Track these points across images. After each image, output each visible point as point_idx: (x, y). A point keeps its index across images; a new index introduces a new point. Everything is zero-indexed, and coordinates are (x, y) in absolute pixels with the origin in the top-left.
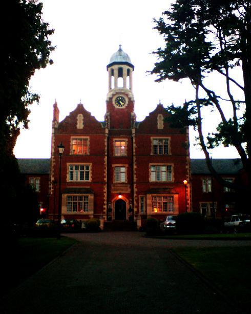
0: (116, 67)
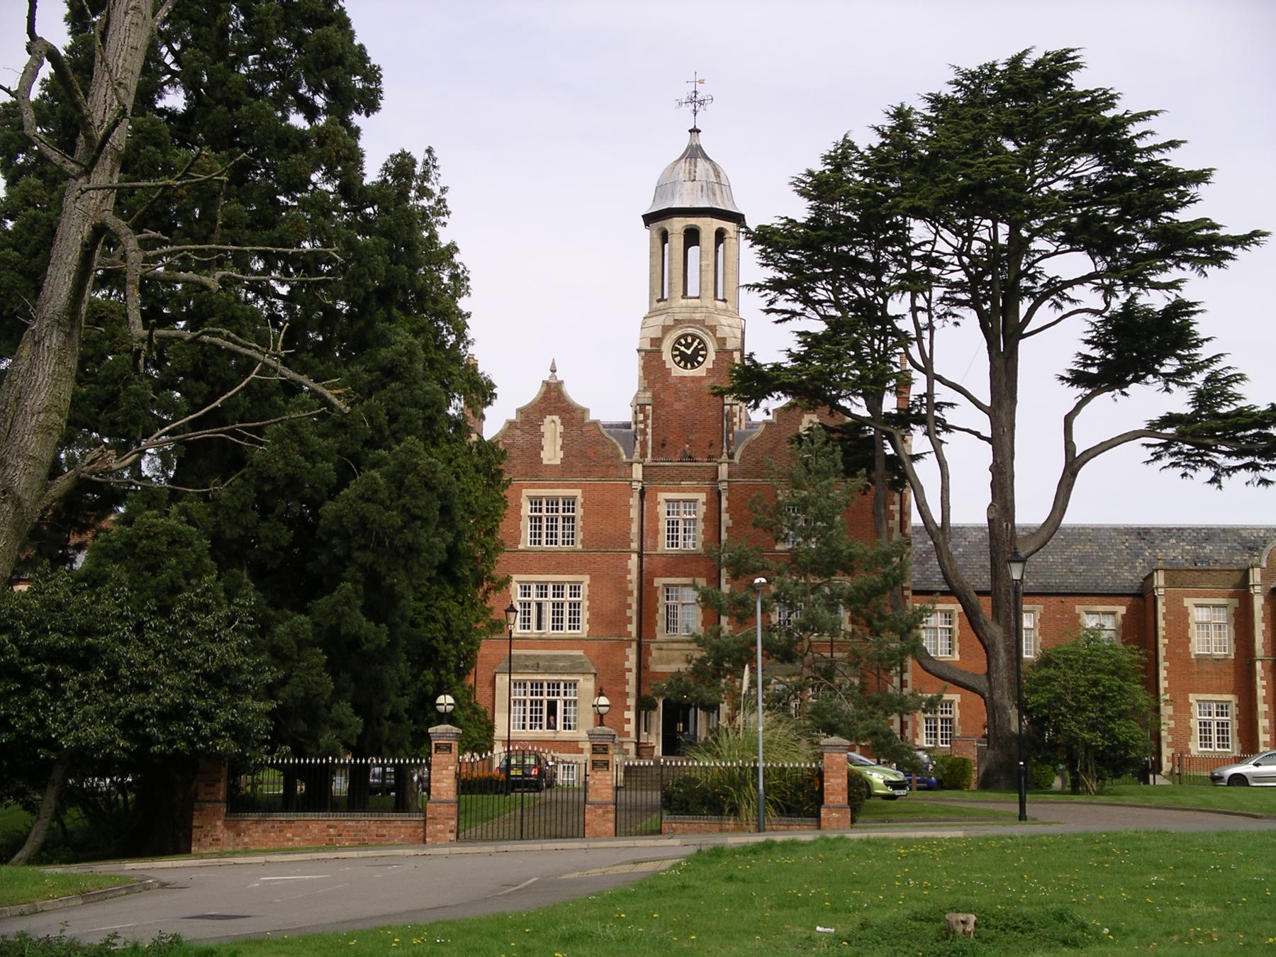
0: (677, 225)
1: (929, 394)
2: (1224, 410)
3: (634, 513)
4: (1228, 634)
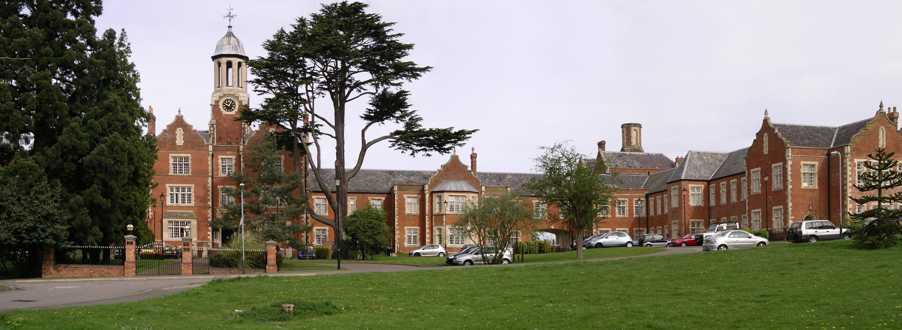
0: (224, 60)
1: (313, 122)
2: (415, 130)
3: (210, 163)
4: (418, 206)
